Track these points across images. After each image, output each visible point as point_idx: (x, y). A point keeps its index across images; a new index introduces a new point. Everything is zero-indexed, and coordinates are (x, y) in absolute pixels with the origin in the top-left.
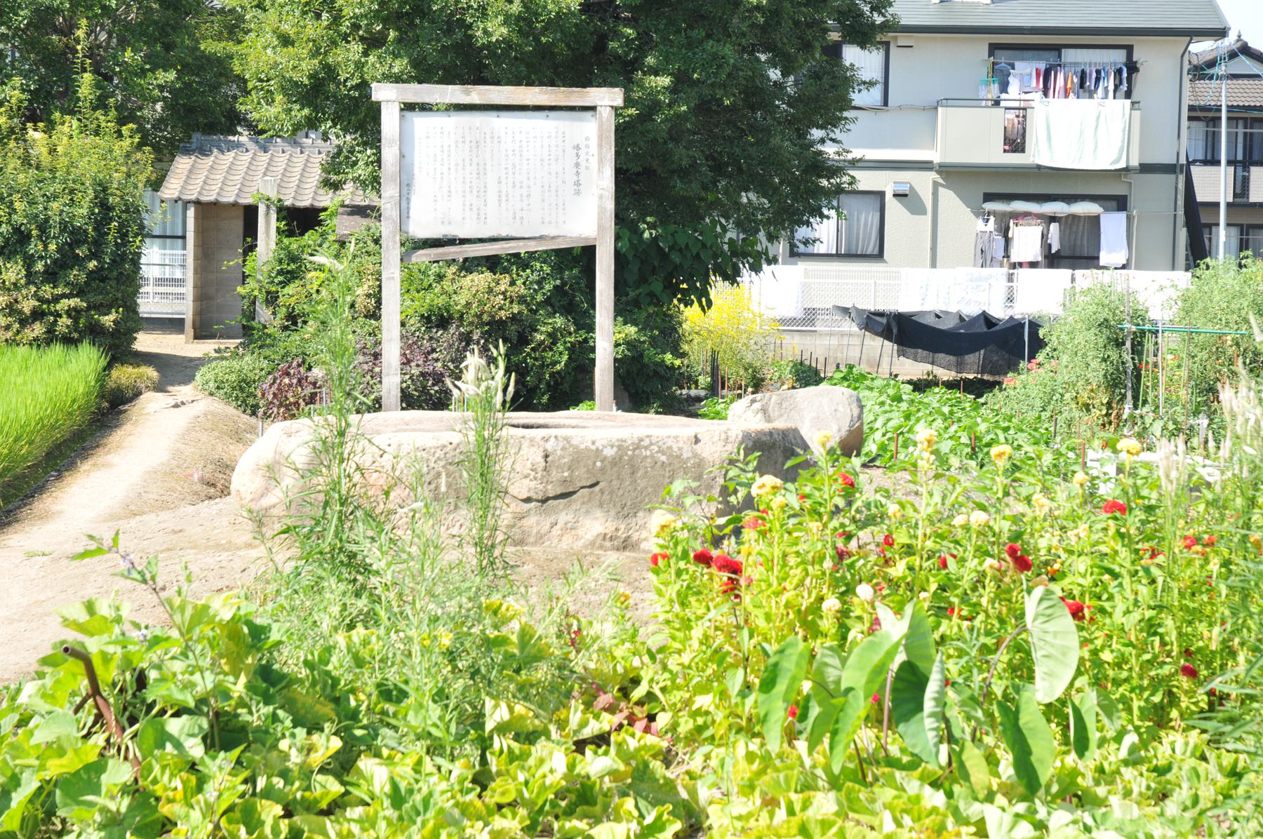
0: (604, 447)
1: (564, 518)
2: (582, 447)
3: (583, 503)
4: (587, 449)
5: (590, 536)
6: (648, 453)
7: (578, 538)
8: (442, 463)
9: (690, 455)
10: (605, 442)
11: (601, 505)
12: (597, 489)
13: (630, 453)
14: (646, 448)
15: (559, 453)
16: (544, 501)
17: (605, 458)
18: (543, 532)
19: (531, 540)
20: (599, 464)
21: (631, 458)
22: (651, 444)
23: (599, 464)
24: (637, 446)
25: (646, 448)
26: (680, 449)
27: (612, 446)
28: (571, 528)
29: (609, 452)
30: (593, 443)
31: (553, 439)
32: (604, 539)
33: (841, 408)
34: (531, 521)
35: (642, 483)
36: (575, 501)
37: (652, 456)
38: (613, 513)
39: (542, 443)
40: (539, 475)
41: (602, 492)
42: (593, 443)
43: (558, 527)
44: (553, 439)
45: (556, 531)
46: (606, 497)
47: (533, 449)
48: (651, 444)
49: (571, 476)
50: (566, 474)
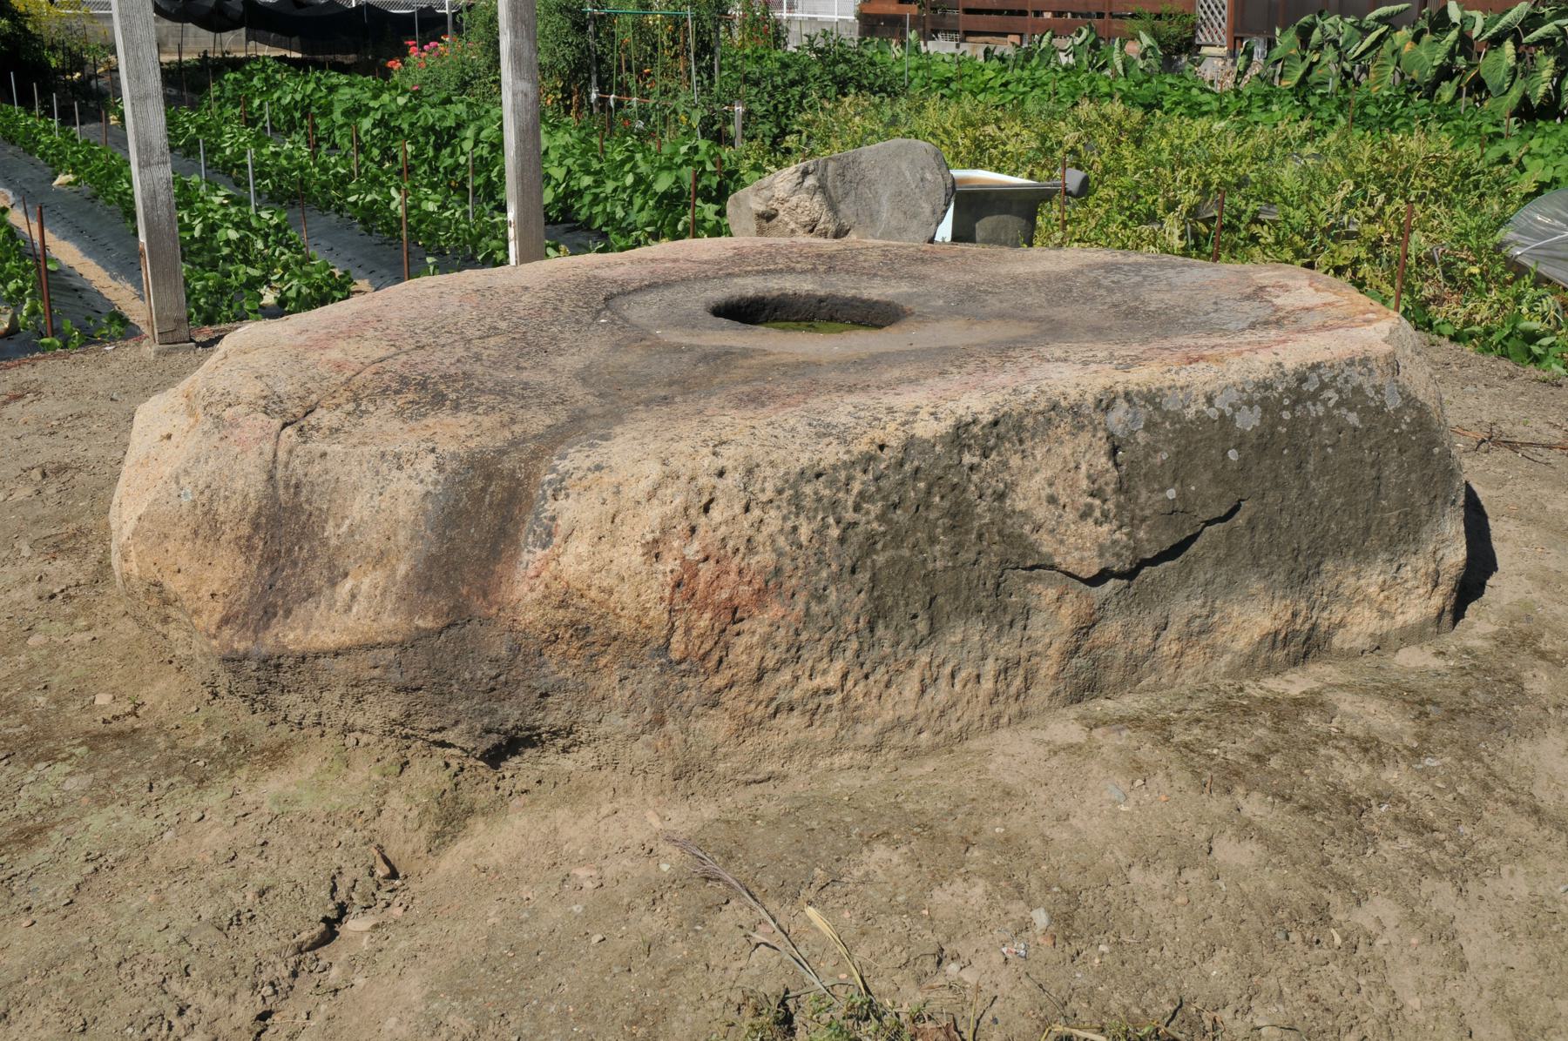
0: (1236, 408)
1: (1184, 609)
2: (1190, 413)
3: (1219, 562)
4: (1201, 417)
5: (1242, 644)
6: (1321, 410)
7: (1214, 652)
8: (875, 509)
9: (1399, 402)
10: (1234, 396)
11: (1256, 562)
12: (1240, 520)
13: (1286, 415)
14: (1314, 397)
15: (1142, 437)
16: (1130, 575)
17: (1243, 435)
18: (1139, 652)
19: (1112, 677)
20: (1233, 455)
21: (1293, 424)
22: (1324, 386)
23: (1233, 455)
24: (1299, 397)
25: (1314, 397)
26: (1378, 390)
27: (1250, 404)
28: (1197, 632)
29: (1249, 420)
30: (1210, 400)
31: (1122, 405)
32: (1273, 646)
33: (928, 176)
34: (1111, 629)
35: (1320, 487)
36: (1199, 559)
37: (1329, 415)
38: (1280, 576)
39: (1098, 417)
40: (1110, 505)
41: (1251, 525)
42: (1210, 400)
43: (1171, 634)
44: (1122, 405)
45: (1169, 647)
46: (1261, 538)
47: (1085, 438)
48: (1324, 386)
49: (1182, 496)
50: (1171, 494)
